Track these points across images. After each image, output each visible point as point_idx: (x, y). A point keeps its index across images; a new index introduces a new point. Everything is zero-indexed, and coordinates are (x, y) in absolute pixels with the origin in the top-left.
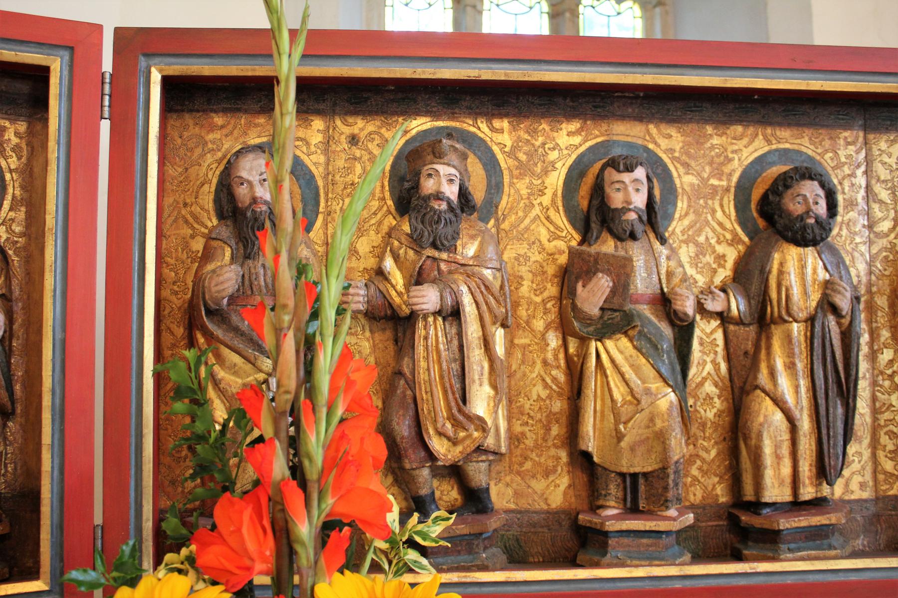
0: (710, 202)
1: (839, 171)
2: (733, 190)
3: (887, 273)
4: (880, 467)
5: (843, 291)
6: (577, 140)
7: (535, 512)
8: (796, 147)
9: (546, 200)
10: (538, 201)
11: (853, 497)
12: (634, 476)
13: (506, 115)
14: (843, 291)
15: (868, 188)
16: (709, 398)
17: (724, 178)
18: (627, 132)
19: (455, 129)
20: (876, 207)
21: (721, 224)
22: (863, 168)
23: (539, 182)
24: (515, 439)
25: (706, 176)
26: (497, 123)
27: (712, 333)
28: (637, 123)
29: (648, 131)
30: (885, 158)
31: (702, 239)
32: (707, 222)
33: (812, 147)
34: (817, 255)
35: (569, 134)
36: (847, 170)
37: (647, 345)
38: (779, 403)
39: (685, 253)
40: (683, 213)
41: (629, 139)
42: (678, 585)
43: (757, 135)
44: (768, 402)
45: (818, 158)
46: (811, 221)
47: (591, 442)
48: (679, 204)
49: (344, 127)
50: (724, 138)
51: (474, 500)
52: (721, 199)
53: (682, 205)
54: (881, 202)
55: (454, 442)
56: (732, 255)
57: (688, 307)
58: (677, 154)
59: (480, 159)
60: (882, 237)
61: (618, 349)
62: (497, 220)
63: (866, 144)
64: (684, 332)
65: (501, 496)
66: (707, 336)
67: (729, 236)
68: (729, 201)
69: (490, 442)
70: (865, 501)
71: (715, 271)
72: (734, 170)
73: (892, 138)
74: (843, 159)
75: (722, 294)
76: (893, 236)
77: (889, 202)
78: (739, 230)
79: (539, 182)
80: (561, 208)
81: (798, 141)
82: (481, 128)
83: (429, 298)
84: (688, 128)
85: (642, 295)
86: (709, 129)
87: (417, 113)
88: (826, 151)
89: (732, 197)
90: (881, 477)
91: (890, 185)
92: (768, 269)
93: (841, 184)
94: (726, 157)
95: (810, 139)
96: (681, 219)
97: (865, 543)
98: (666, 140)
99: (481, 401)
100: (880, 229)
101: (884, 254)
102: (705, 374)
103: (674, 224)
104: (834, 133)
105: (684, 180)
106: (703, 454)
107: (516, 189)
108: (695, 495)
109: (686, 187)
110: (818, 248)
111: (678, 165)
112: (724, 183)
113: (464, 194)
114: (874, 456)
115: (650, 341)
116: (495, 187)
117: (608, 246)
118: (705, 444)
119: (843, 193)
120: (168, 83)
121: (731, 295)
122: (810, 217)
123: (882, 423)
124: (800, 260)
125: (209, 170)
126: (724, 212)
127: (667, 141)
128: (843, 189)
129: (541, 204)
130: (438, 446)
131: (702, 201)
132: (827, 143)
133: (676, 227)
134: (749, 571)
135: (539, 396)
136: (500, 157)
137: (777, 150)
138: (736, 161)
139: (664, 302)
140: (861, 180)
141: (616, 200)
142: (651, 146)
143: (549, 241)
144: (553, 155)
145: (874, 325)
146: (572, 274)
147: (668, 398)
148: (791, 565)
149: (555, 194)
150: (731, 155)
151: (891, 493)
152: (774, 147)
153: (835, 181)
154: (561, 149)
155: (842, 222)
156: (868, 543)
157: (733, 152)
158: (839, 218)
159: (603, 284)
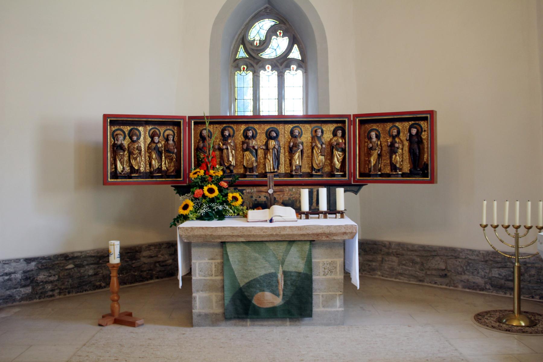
18: (251, 125)
24: (236, 164)
37: (251, 152)
39: (258, 141)
47: (245, 164)
49: (215, 126)
51: (231, 171)
56: (265, 141)
57: (256, 148)
61: (247, 153)
64: (256, 151)
65: (235, 171)
66: (259, 152)
82: (232, 126)
83: (224, 147)
98: (256, 126)
99: (231, 159)
105: (258, 131)
107: (236, 133)
113: (229, 134)
116: (234, 133)
117: (247, 141)
120: (194, 122)
125: (199, 132)
130: (226, 164)
133: (258, 137)
139: (253, 147)
140: (283, 130)
146: (243, 143)
147: (254, 159)
159: (246, 145)
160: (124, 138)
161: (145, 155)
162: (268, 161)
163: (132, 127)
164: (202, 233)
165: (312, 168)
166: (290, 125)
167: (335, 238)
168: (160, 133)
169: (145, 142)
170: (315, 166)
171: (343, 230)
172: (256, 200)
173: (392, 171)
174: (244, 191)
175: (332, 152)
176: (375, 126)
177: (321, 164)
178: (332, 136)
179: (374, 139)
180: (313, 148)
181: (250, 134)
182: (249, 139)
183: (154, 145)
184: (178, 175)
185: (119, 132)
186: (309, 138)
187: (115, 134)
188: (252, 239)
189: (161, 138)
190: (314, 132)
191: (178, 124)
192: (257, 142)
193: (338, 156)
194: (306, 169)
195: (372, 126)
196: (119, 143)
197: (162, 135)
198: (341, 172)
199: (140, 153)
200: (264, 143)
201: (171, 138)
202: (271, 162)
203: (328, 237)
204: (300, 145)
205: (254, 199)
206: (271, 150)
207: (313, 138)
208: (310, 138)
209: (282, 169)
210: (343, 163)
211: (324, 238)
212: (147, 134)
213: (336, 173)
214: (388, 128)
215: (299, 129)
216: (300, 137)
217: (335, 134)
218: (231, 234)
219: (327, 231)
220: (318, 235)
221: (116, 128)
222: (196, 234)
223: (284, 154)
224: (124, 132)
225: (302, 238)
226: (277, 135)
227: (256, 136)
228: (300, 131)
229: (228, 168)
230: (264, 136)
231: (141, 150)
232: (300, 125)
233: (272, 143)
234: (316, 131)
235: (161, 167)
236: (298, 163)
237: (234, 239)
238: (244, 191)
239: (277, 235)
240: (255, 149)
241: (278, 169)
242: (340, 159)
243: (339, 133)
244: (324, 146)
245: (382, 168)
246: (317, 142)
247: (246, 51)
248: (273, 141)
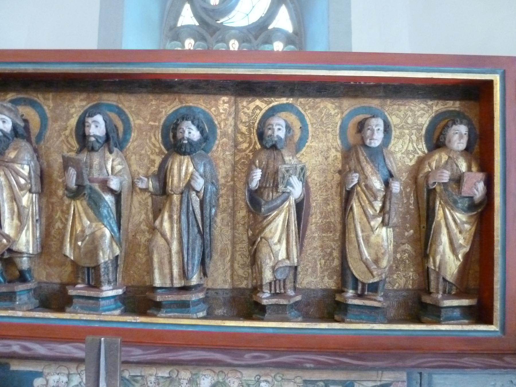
0: (149, 133)
1: (218, 117)
2: (161, 127)
3: (243, 170)
4: (235, 273)
5: (196, 178)
6: (84, 103)
7: (54, 283)
8: (196, 105)
9: (67, 132)
10: (64, 133)
11: (218, 287)
12: (88, 268)
13: (51, 92)
14: (196, 178)
15: (236, 125)
16: (143, 232)
17: (157, 121)
19: (27, 99)
20: (239, 136)
21: (154, 145)
22: (233, 116)
23: (65, 124)
25: (147, 120)
26: (47, 96)
27: (146, 199)
28: (114, 94)
29: (119, 99)
30: (246, 110)
31: (143, 152)
32: (147, 143)
33: (204, 105)
34: (190, 160)
35: (81, 100)
36: (223, 116)
37: (95, 204)
38: (163, 236)
40: (134, 139)
41: (110, 102)
42: (97, 325)
43: (175, 99)
44: (159, 235)
45: (207, 110)
46: (186, 142)
48: (133, 134)
50: (158, 101)
52: (155, 132)
53: (134, 135)
54: (242, 133)
56: (158, 160)
58: (133, 109)
59: (38, 112)
60: (242, 152)
62: (44, 141)
63: (235, 103)
67: (157, 150)
68: (159, 133)
70: (226, 289)
71: (149, 168)
72: (162, 117)
73: (250, 100)
74: (221, 111)
75: (146, 179)
76: (248, 151)
77: (247, 133)
78: (163, 147)
79: (65, 124)
80: (74, 136)
81: (197, 102)
82: (39, 98)
84: (139, 96)
85: (96, 178)
86: (151, 97)
87: (12, 91)
88: (212, 107)
89: (160, 131)
90: (235, 278)
91: (247, 124)
92: (166, 167)
93: (219, 124)
94: (159, 110)
95: (204, 101)
96: (133, 141)
97: (225, 311)
100: (241, 147)
101: (243, 160)
102: (141, 220)
103: (130, 144)
104: (217, 97)
105: (135, 121)
106: (140, 260)
107: (53, 127)
108: (134, 280)
109: (136, 126)
110: (192, 156)
111: (133, 115)
112: (157, 124)
114: (232, 266)
115: (94, 201)
118: (140, 255)
119: (221, 128)
121: (150, 180)
122: (185, 140)
123: (238, 249)
124: (180, 162)
126: (156, 138)
127: (128, 103)
128: (220, 127)
129: (65, 134)
131: (144, 133)
132: (213, 102)
133: (131, 145)
134: (133, 321)
135: (59, 227)
136: (47, 111)
137: (185, 107)
138: (164, 113)
140: (231, 121)
142: (120, 106)
143: (68, 152)
144: (73, 110)
145: (235, 198)
148: (163, 320)
149: (71, 130)
150: (161, 110)
151: (241, 286)
152: (184, 105)
153: (216, 122)
154: (76, 108)
155: (219, 144)
156: (227, 311)
157: (162, 108)
158: (217, 142)
162: (160, 241)
166: (258, 102)
170: (357, 269)
175: (429, 215)
177: (384, 263)
178: (422, 148)
181: (97, 128)
182: (93, 150)
186: (333, 153)
190: (351, 131)
192: (127, 159)
194: (317, 279)
198: (459, 295)
200: (155, 169)
202: (175, 246)
204: (294, 180)
206: (176, 198)
207: (349, 153)
208: (335, 154)
209: (221, 277)
213: (448, 303)
215: (293, 119)
216: (298, 149)
217: (436, 141)
223: (233, 215)
226: (207, 138)
227: (125, 140)
228: (297, 125)
230: (156, 140)
232: (301, 103)
233: (182, 168)
234: (361, 126)
236: (282, 255)
240: (112, 191)
242: (463, 241)
243: (459, 136)
244: (396, 187)
246: (368, 169)
247: (196, 15)
248: (186, 160)
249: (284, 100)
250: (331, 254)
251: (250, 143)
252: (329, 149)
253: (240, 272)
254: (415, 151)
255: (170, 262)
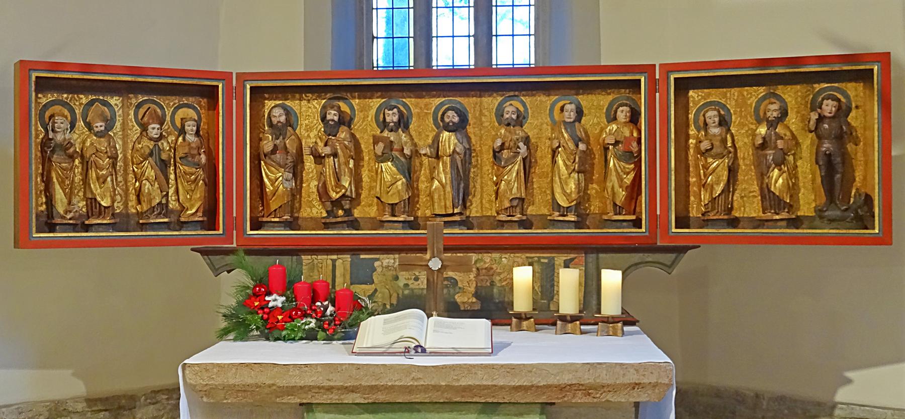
9: (369, 119)
15: (481, 111)
55: (337, 193)
69: (348, 193)
105: (414, 111)
114: (481, 202)
120: (251, 88)
141: (388, 119)
160: (73, 126)
161: (125, 170)
163: (91, 97)
164: (250, 381)
165: (556, 206)
167: (609, 397)
168: (164, 115)
169: (125, 137)
171: (633, 378)
172: (406, 285)
173: (764, 213)
174: (377, 264)
176: (715, 95)
179: (715, 130)
180: (554, 152)
181: (392, 117)
183: (147, 144)
184: (211, 224)
185: (57, 108)
187: (47, 114)
188: (381, 397)
189: (165, 127)
191: (210, 93)
193: (618, 174)
195: (709, 95)
196: (59, 137)
197: (168, 118)
199: (114, 165)
200: (430, 141)
201: (190, 127)
203: (589, 394)
205: (401, 283)
210: (634, 189)
211: (580, 398)
212: (132, 116)
214: (753, 101)
218: (326, 384)
219: (588, 379)
220: (562, 388)
221: (50, 97)
222: (231, 382)
224: (72, 111)
225: (519, 397)
229: (337, 203)
231: (116, 158)
235: (167, 201)
236: (514, 190)
237: (334, 398)
238: (377, 264)
239: (449, 388)
241: (465, 207)
242: (628, 179)
243: (623, 114)
245: (735, 205)
249: (512, 93)
250: (545, 192)
251: (491, 122)
252: (542, 124)
253: (487, 205)
254: (599, 123)
255: (445, 199)
